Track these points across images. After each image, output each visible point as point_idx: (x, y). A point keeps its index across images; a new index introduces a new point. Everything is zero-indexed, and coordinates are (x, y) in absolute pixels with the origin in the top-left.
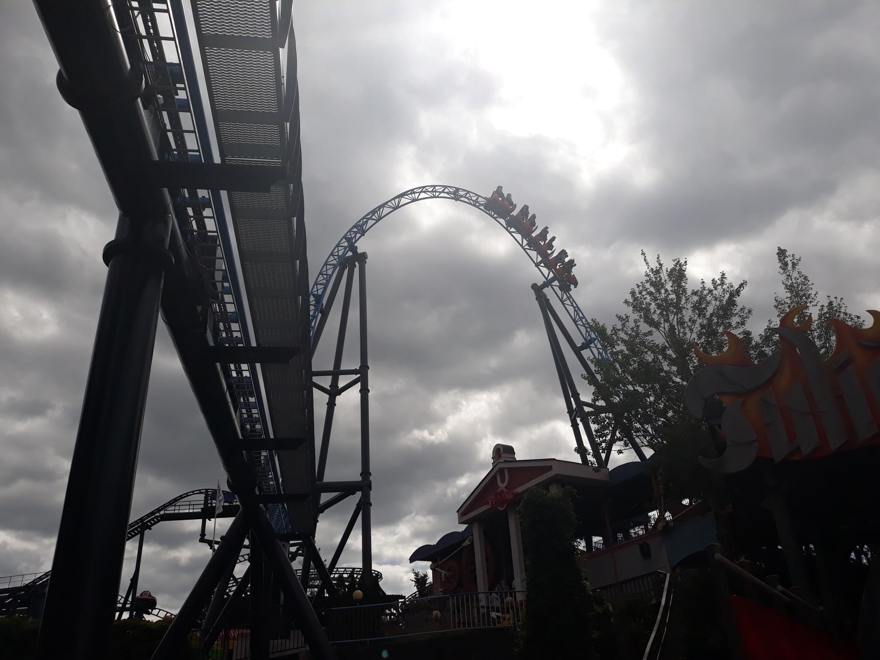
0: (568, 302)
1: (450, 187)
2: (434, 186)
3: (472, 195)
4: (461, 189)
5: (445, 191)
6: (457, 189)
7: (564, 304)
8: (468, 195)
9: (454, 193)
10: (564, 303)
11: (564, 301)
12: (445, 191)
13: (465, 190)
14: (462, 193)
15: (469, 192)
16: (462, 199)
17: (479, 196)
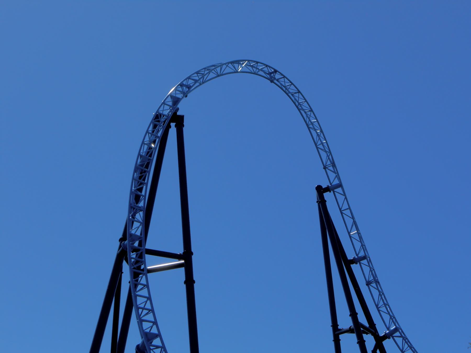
0: (383, 309)
1: (270, 67)
2: (257, 62)
3: (286, 80)
4: (279, 72)
5: (263, 70)
6: (276, 71)
7: (379, 311)
8: (282, 80)
9: (270, 74)
10: (379, 309)
11: (379, 308)
12: (263, 70)
13: (282, 75)
14: (277, 76)
15: (284, 77)
16: (275, 81)
17: (292, 84)
